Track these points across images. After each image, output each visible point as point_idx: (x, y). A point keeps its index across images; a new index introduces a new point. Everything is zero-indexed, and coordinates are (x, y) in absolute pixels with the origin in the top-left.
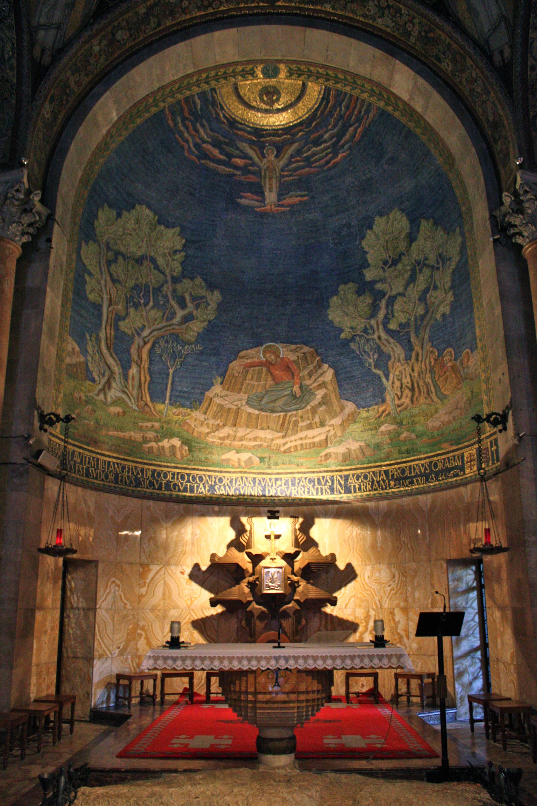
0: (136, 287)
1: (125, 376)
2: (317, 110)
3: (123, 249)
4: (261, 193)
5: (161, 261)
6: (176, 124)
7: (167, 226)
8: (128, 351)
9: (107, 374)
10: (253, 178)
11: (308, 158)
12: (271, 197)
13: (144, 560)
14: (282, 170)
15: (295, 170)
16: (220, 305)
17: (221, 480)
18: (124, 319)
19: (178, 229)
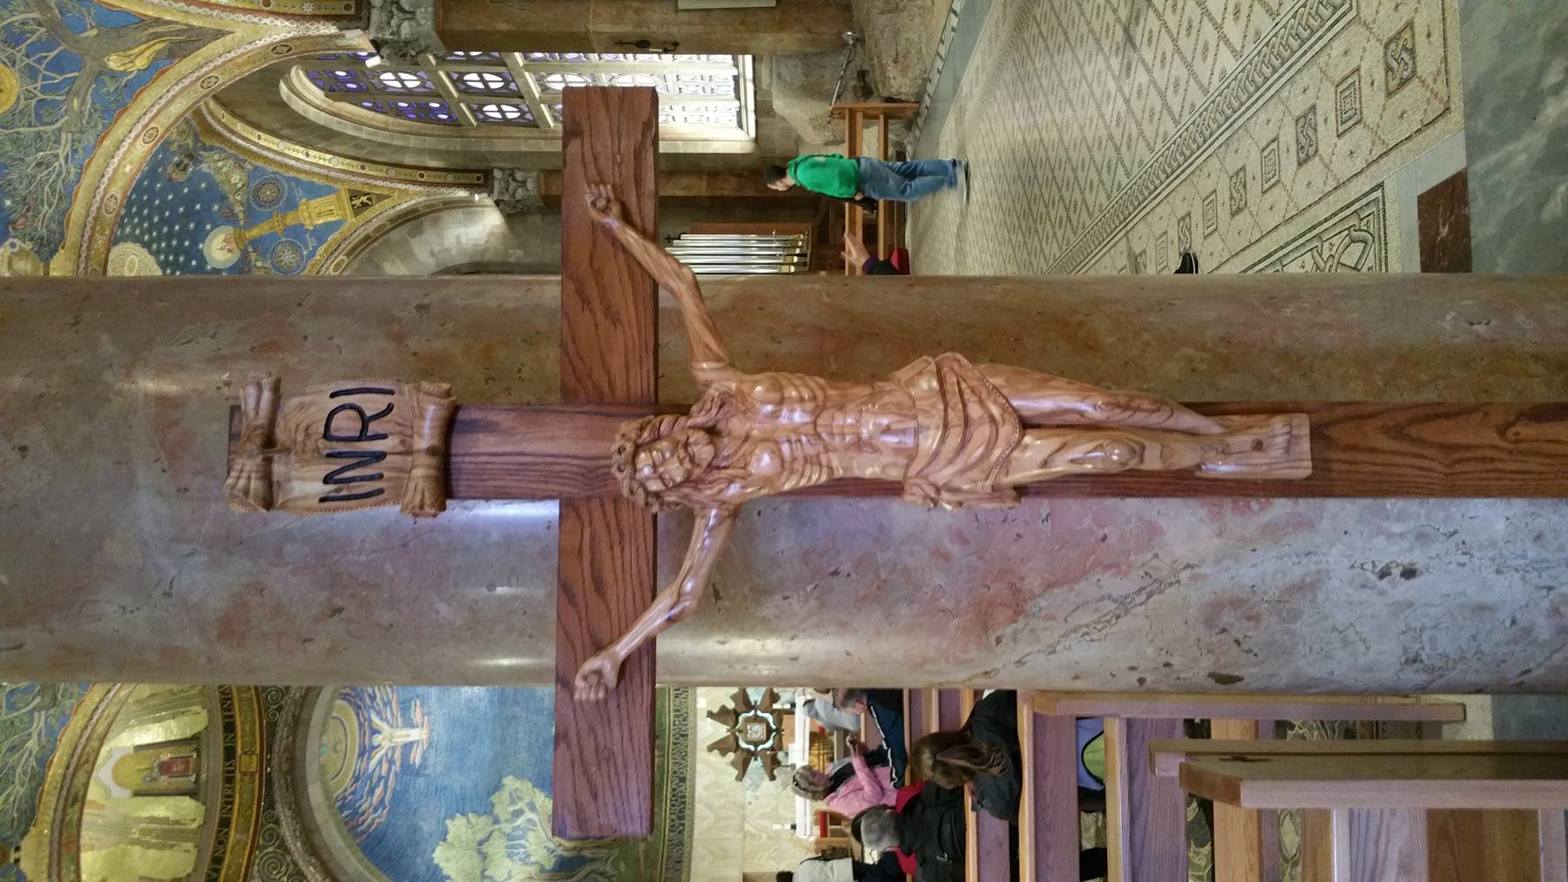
0: (510, 856)
1: (593, 860)
2: (350, 702)
3: (478, 871)
4: (412, 743)
5: (480, 836)
6: (363, 832)
7: (446, 833)
8: (571, 860)
9: (594, 876)
10: (397, 755)
11: (385, 704)
12: (415, 734)
13: (740, 836)
14: (392, 726)
15: (393, 715)
16: (517, 777)
17: (675, 772)
18: (542, 866)
19: (448, 822)
